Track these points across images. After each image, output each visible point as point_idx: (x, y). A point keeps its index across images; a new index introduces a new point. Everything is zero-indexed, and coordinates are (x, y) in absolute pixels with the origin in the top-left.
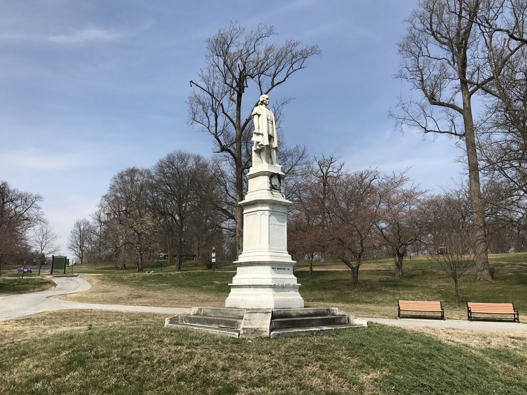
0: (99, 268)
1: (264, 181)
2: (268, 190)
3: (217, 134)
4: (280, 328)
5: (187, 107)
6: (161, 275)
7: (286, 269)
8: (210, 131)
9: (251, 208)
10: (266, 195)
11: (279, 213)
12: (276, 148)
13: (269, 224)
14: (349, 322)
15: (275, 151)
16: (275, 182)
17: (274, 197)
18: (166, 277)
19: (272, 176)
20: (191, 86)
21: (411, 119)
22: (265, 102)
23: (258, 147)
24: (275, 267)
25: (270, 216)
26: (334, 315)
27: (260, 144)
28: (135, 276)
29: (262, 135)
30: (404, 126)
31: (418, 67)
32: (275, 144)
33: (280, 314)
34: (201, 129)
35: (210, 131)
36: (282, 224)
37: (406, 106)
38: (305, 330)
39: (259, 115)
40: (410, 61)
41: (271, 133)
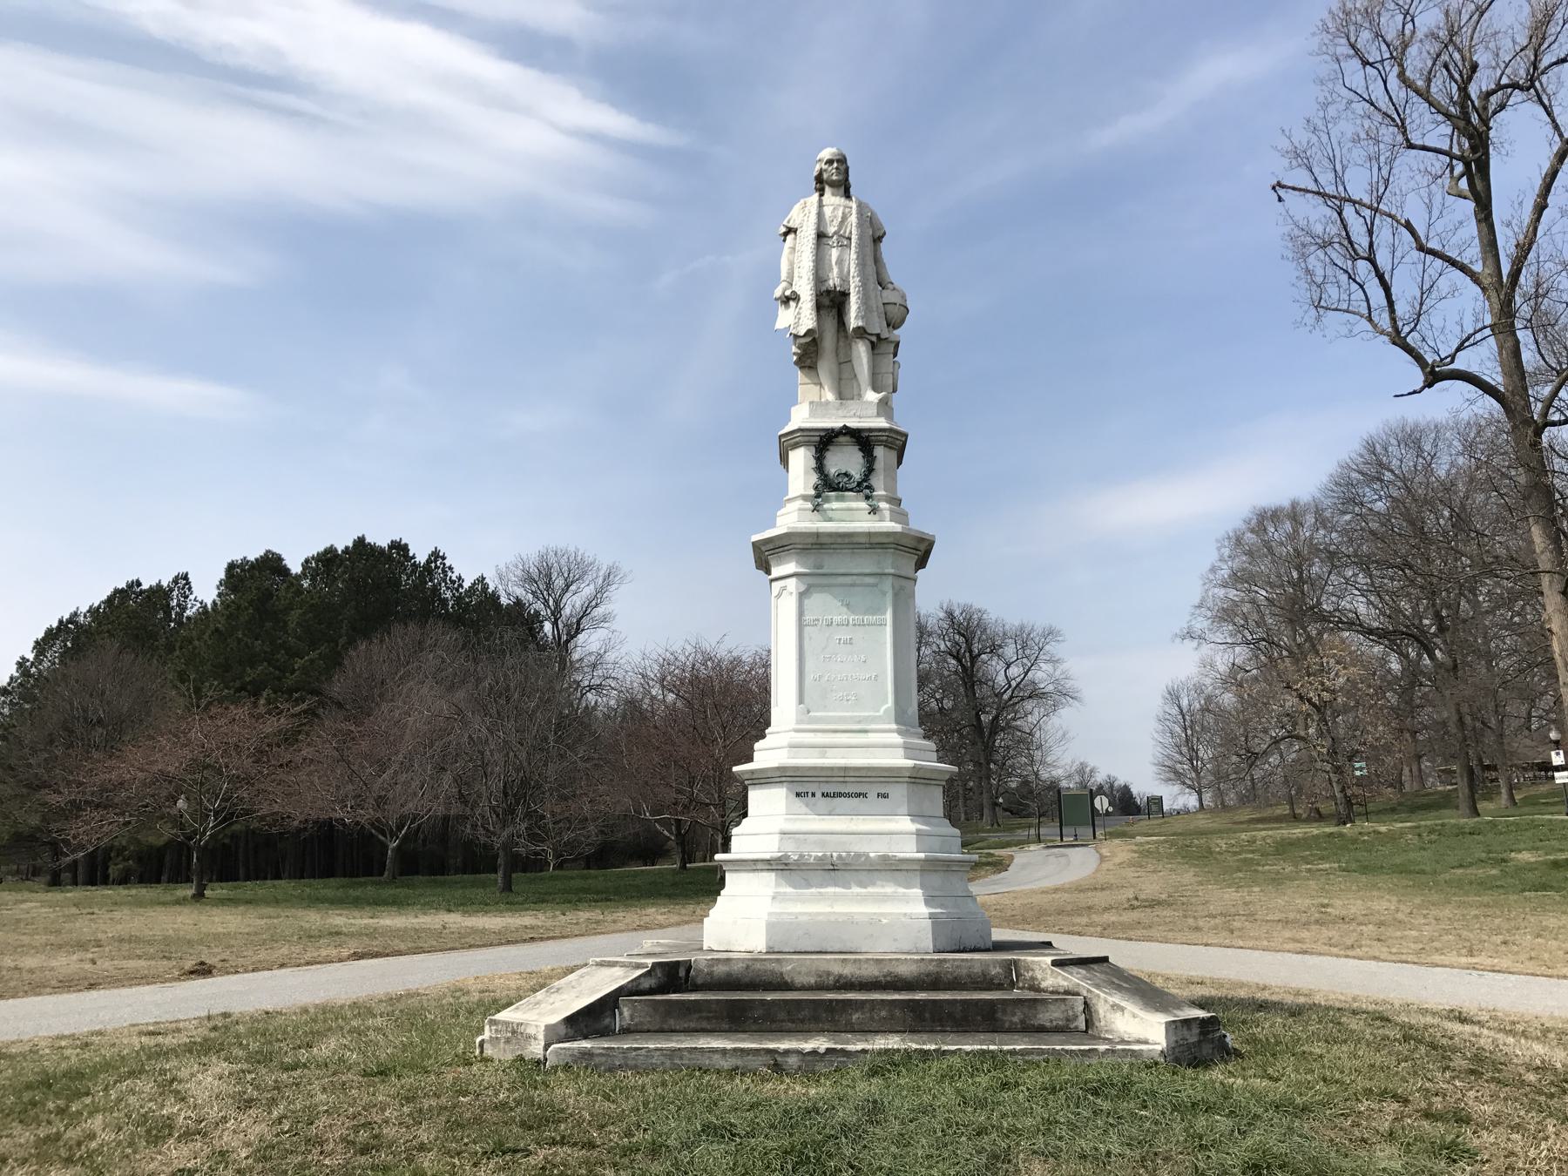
0: (1243, 818)
2: (805, 498)
3: (1398, 332)
4: (661, 1031)
5: (1292, 271)
6: (1341, 835)
7: (872, 795)
8: (1375, 326)
11: (848, 580)
14: (1089, 1023)
16: (846, 460)
17: (830, 520)
18: (1354, 841)
20: (1280, 199)
24: (810, 788)
25: (802, 596)
26: (1035, 988)
28: (1252, 841)
33: (729, 975)
34: (1344, 331)
35: (1375, 326)
38: (729, 1045)
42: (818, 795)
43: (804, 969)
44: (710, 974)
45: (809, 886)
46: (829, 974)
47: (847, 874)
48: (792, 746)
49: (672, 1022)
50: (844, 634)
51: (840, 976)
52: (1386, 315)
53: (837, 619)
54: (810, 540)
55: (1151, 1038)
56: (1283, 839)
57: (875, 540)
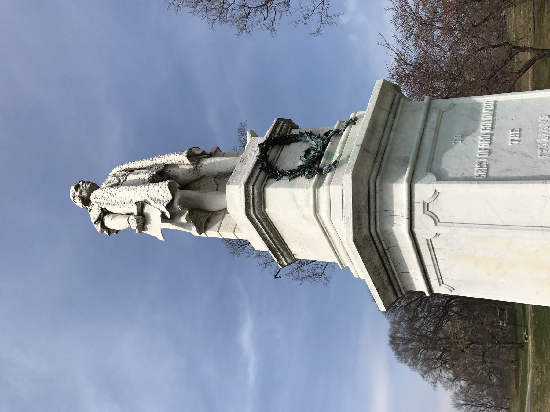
0: (515, 392)
1: (286, 201)
2: (318, 185)
9: (400, 263)
10: (338, 192)
12: (190, 156)
13: (488, 179)
15: (208, 162)
16: (293, 156)
18: (538, 326)
19: (268, 169)
20: (280, 277)
21: (321, 5)
22: (84, 194)
23: (183, 220)
25: (441, 177)
27: (168, 214)
29: (141, 205)
30: (330, 12)
31: (263, 6)
32: (179, 159)
36: (485, 115)
37: (307, 12)
39: (105, 212)
40: (256, 17)
41: (147, 175)
54: (369, 161)
57: (387, 106)
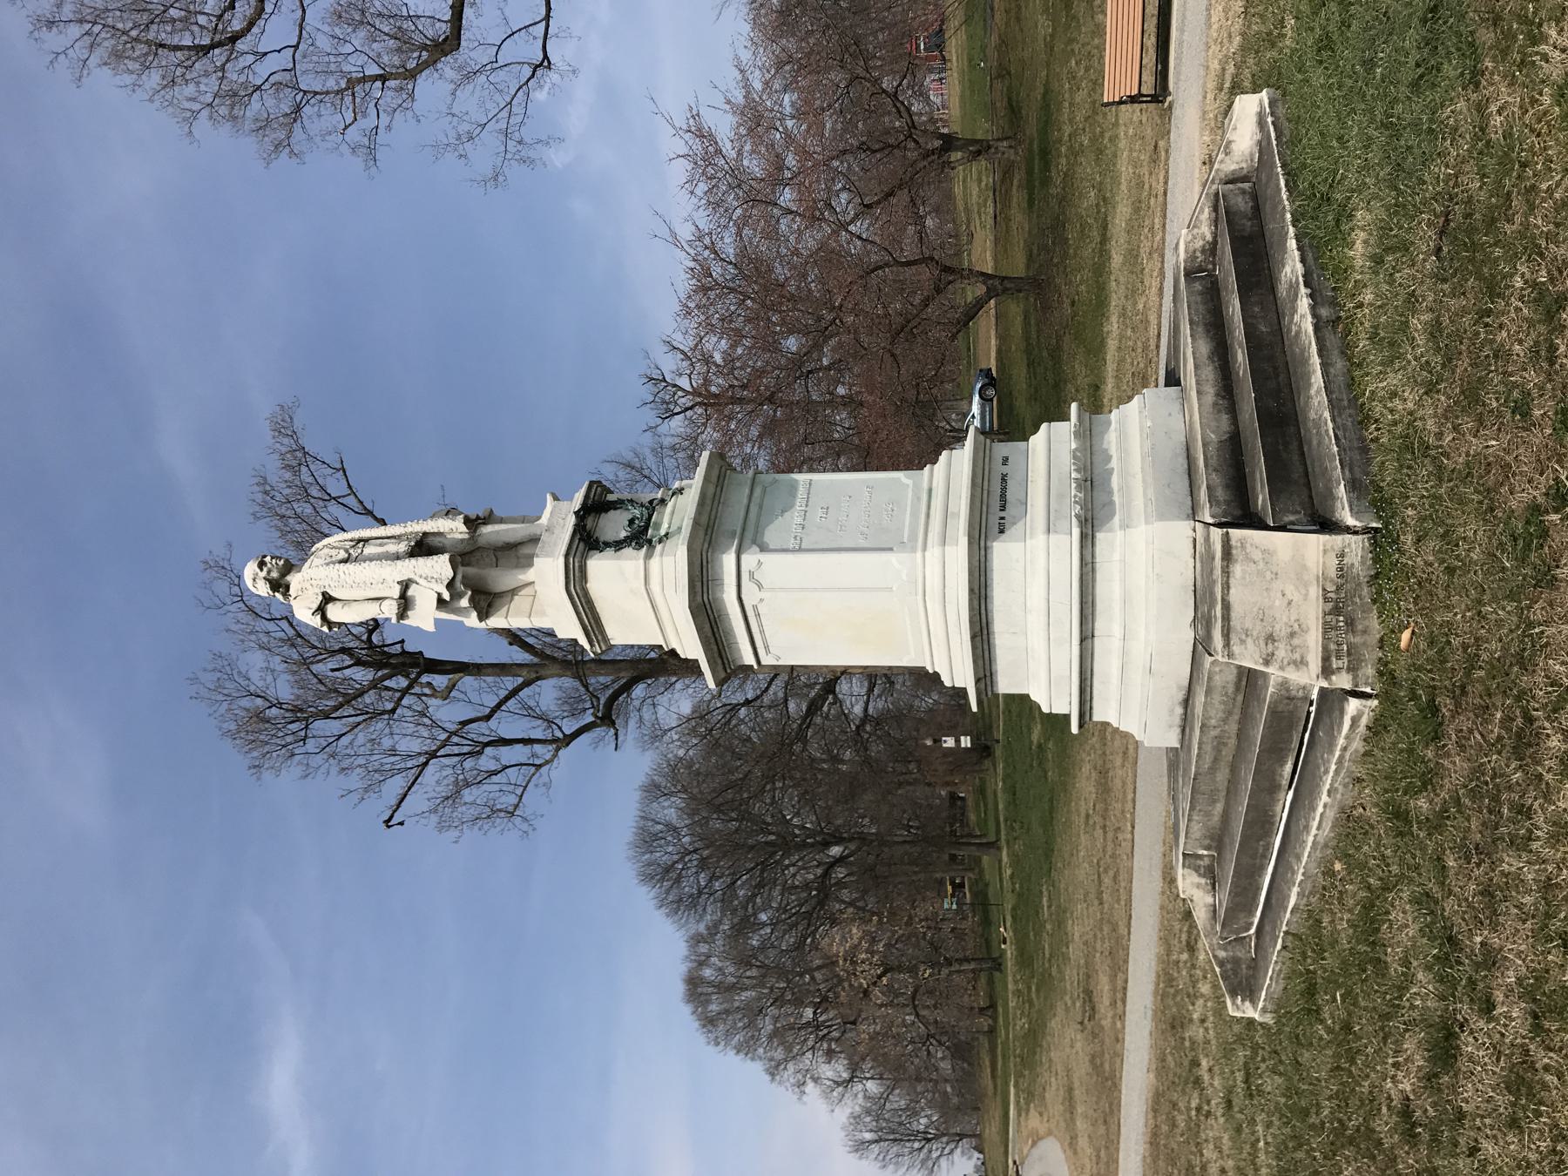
0: (991, 1087)
1: (609, 574)
2: (648, 556)
3: (554, 741)
4: (1308, 485)
5: (471, 834)
6: (1014, 909)
7: (1005, 470)
8: (547, 762)
9: (730, 633)
10: (671, 565)
11: (754, 509)
12: (468, 521)
13: (800, 550)
14: (1245, 179)
15: (487, 530)
16: (614, 525)
17: (680, 528)
18: (1020, 895)
19: (586, 540)
20: (401, 824)
21: (505, 114)
22: (275, 575)
23: (464, 602)
24: (994, 521)
25: (764, 549)
26: (1212, 249)
27: (446, 596)
28: (1018, 993)
29: (405, 585)
30: (527, 133)
31: (340, 92)
32: (454, 528)
33: (1227, 486)
34: (543, 789)
35: (547, 762)
36: (801, 492)
37: (464, 127)
38: (1316, 360)
39: (327, 599)
40: (321, 119)
41: (402, 547)
42: (1003, 514)
43: (1214, 424)
44: (1228, 503)
45: (1112, 503)
46: (1215, 404)
47: (1096, 472)
48: (944, 543)
49: (1295, 476)
50: (816, 514)
51: (1217, 395)
52: (537, 748)
53: (799, 520)
54: (701, 533)
55: (1256, 109)
56: (1017, 963)
57: (714, 479)
